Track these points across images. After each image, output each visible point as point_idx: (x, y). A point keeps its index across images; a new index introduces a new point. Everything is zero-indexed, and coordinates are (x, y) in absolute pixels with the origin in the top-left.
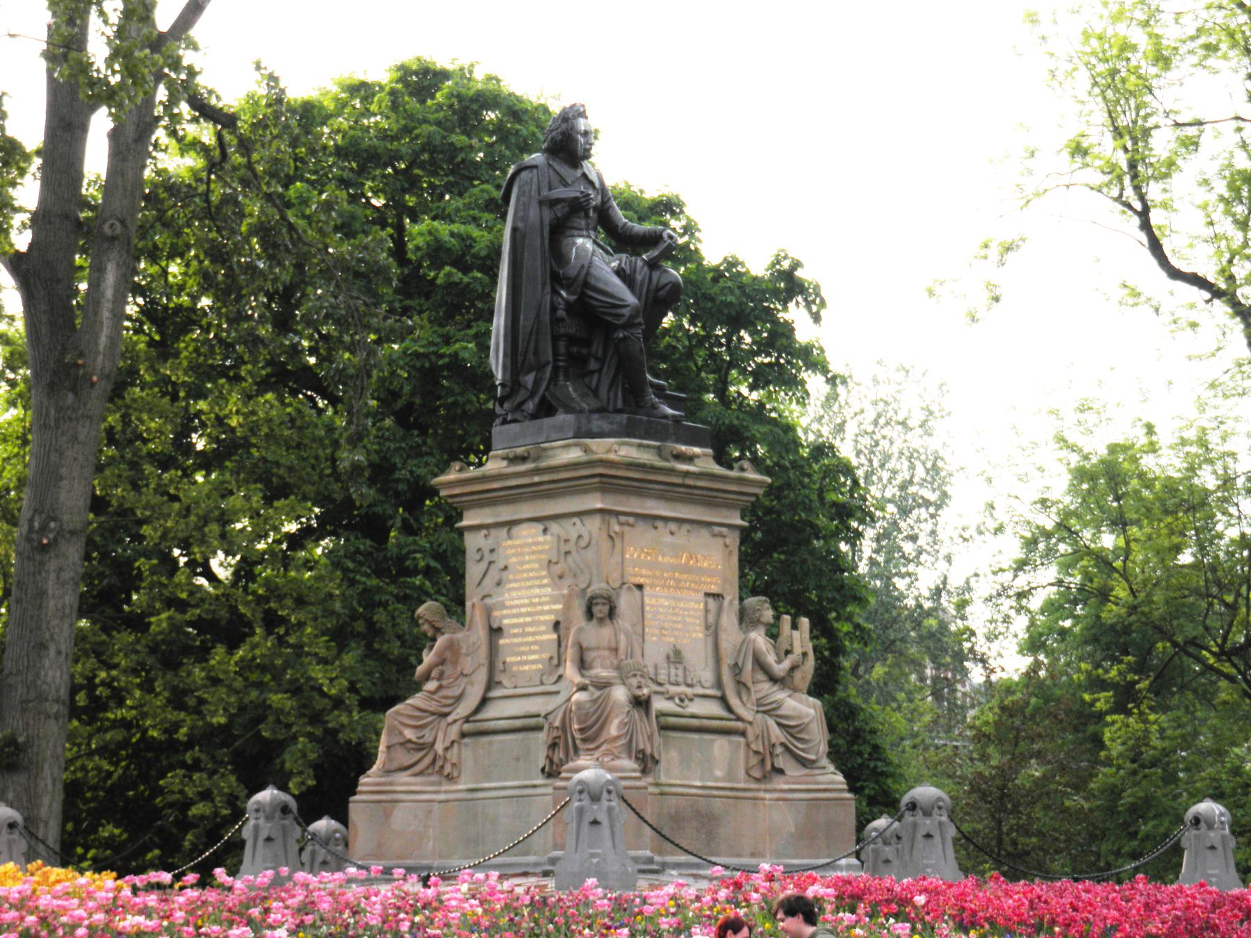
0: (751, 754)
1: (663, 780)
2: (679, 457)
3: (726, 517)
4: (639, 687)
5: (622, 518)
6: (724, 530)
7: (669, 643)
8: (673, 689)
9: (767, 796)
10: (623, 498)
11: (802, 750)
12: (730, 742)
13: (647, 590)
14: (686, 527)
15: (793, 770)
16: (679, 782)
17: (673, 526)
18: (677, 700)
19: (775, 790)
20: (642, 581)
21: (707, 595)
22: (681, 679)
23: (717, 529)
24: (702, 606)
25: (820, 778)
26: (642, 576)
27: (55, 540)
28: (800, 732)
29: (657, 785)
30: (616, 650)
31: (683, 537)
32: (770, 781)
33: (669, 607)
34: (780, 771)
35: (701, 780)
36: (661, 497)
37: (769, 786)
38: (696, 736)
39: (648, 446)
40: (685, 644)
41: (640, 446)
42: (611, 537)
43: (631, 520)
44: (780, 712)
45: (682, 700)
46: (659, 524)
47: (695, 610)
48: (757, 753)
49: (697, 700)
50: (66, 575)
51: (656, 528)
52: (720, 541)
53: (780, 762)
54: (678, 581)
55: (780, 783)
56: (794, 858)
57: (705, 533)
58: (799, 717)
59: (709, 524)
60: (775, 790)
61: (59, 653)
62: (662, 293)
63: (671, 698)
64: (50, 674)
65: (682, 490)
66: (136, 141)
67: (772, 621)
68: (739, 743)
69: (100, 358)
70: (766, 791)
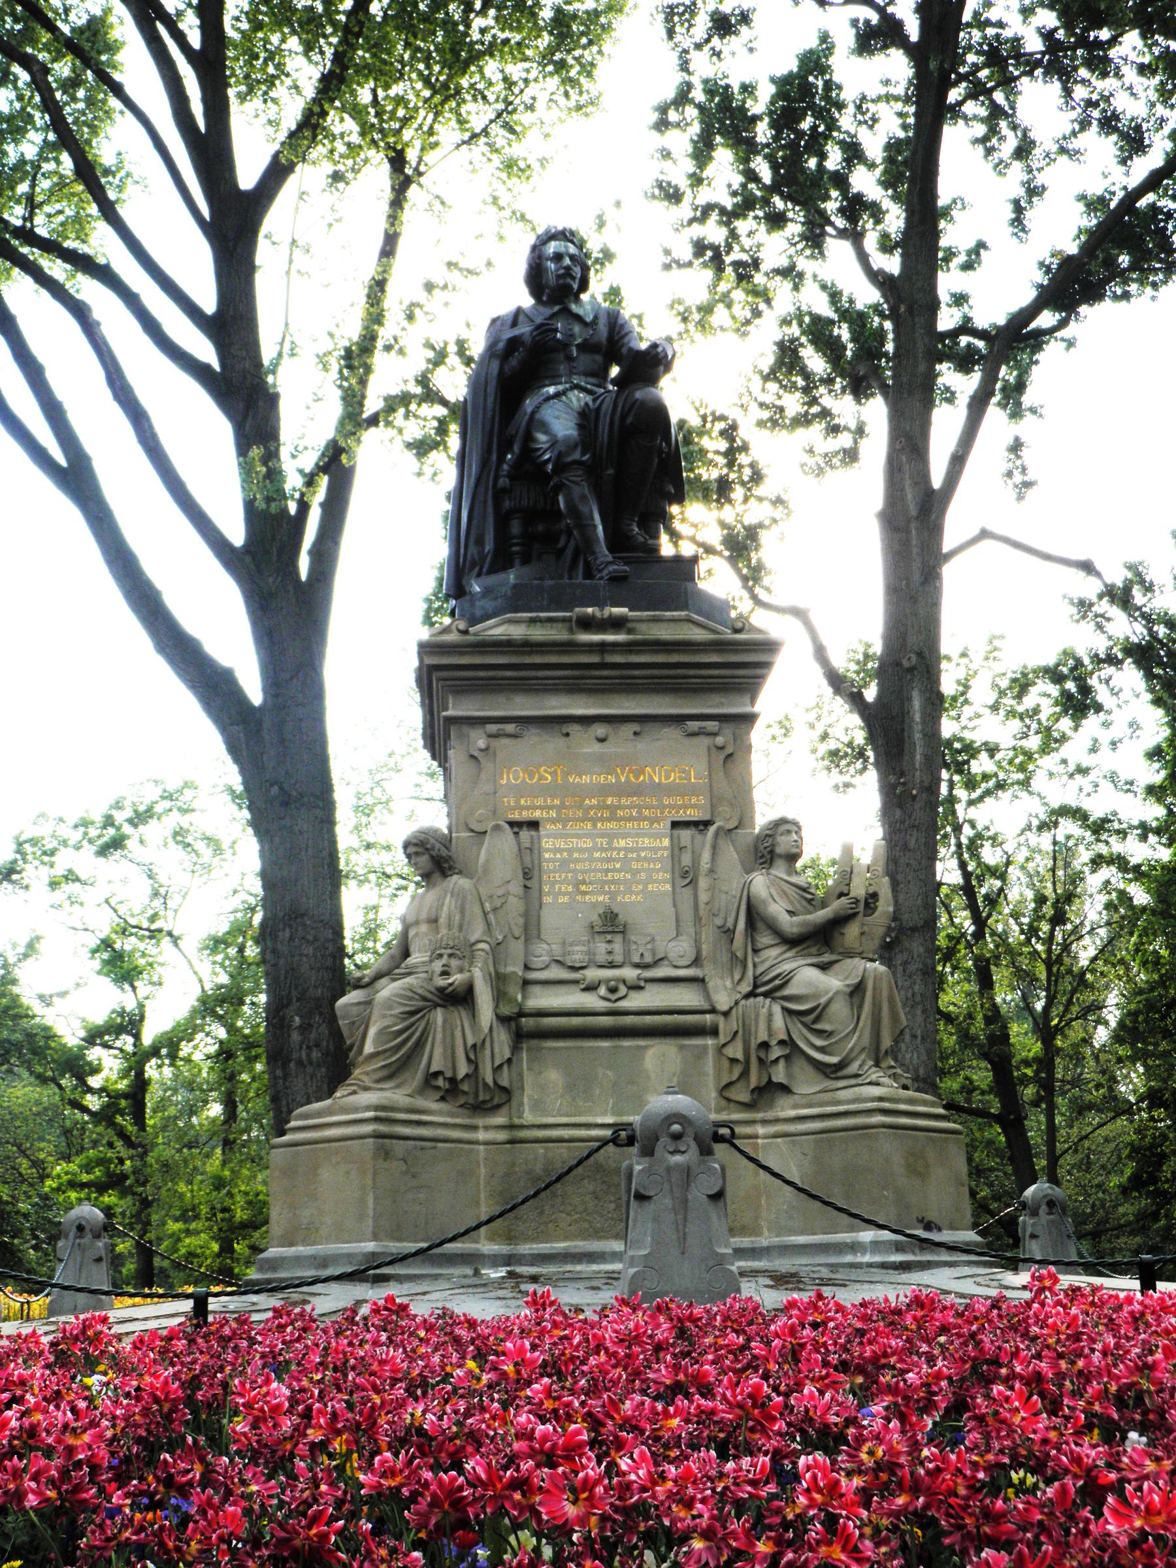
0: (726, 1064)
1: (529, 1117)
2: (587, 624)
3: (717, 706)
4: (445, 973)
5: (492, 728)
6: (712, 725)
7: (594, 905)
8: (592, 974)
9: (761, 1130)
10: (501, 699)
11: (821, 1050)
12: (682, 1047)
13: (547, 829)
14: (628, 729)
15: (807, 1085)
16: (564, 1120)
17: (600, 730)
18: (602, 991)
19: (777, 1121)
20: (537, 814)
21: (675, 825)
22: (618, 958)
23: (694, 725)
24: (666, 842)
25: (842, 1095)
26: (535, 808)
27: (897, 937)
28: (817, 1020)
29: (511, 1127)
30: (436, 921)
31: (622, 741)
32: (771, 1105)
33: (595, 848)
34: (785, 1089)
35: (613, 1114)
36: (573, 687)
37: (769, 1115)
38: (605, 1044)
39: (551, 620)
40: (629, 901)
41: (532, 621)
42: (472, 756)
43: (510, 728)
44: (786, 992)
45: (613, 990)
46: (574, 729)
47: (655, 850)
48: (733, 1061)
49: (649, 986)
50: (912, 967)
51: (567, 735)
52: (706, 741)
53: (779, 1074)
54: (613, 808)
55: (785, 1108)
56: (802, 1233)
57: (671, 734)
58: (816, 996)
59: (680, 719)
60: (777, 1121)
61: (914, 1036)
62: (629, 420)
63: (591, 988)
64: (908, 1056)
65: (606, 673)
66: (923, 584)
67: (779, 850)
68: (705, 1047)
69: (918, 773)
70: (764, 1122)
